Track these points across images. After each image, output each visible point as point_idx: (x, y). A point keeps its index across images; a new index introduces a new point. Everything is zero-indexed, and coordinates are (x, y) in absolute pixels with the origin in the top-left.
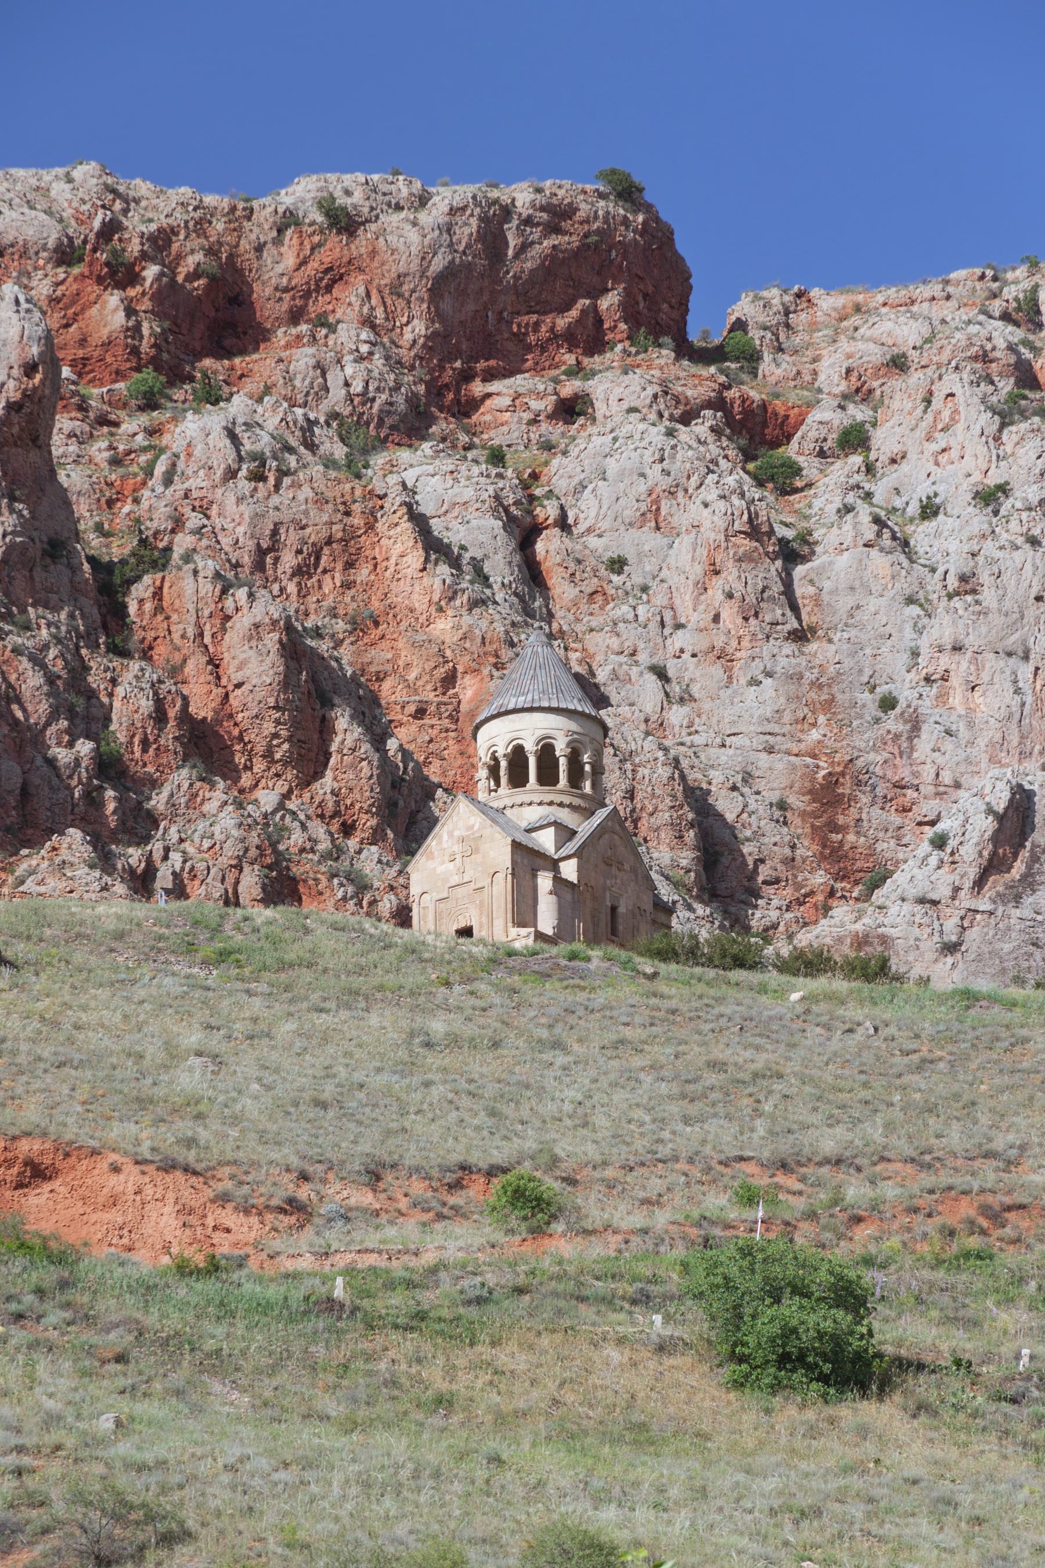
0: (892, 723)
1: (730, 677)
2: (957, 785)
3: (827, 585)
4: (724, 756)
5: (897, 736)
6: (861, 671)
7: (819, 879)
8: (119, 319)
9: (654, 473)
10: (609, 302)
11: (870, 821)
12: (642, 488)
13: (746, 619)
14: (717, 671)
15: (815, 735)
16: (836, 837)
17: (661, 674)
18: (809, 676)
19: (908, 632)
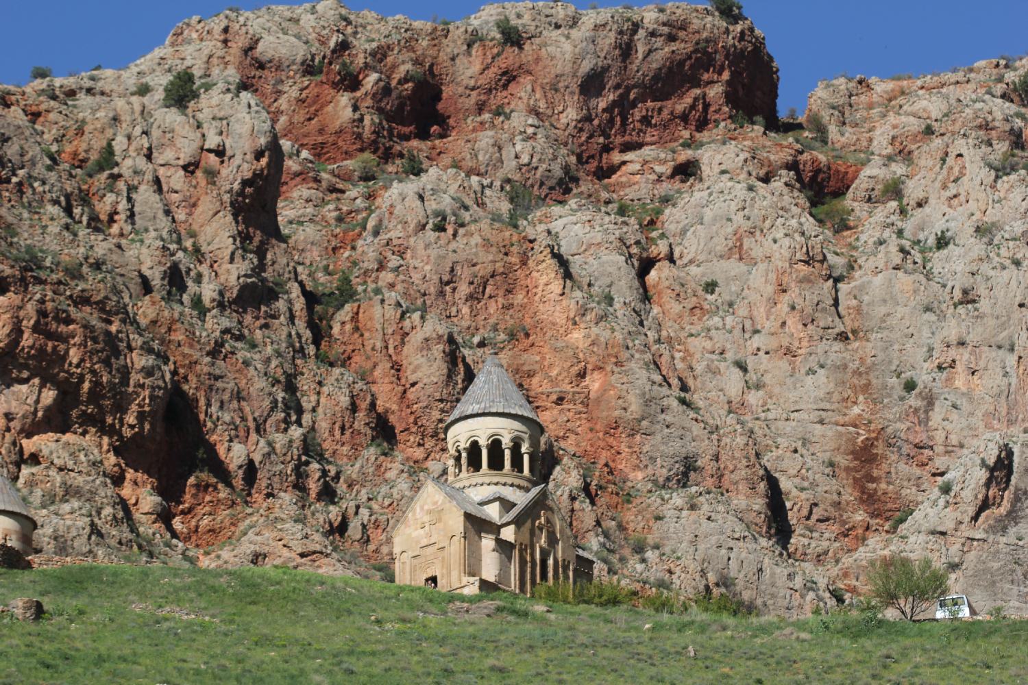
0: (913, 401)
1: (793, 369)
2: (961, 446)
3: (866, 298)
4: (788, 427)
5: (916, 410)
6: (890, 362)
7: (860, 517)
8: (348, 114)
9: (738, 219)
10: (715, 92)
11: (898, 472)
12: (730, 229)
13: (805, 325)
14: (784, 364)
15: (856, 410)
16: (872, 486)
17: (743, 367)
18: (852, 366)
19: (926, 333)
